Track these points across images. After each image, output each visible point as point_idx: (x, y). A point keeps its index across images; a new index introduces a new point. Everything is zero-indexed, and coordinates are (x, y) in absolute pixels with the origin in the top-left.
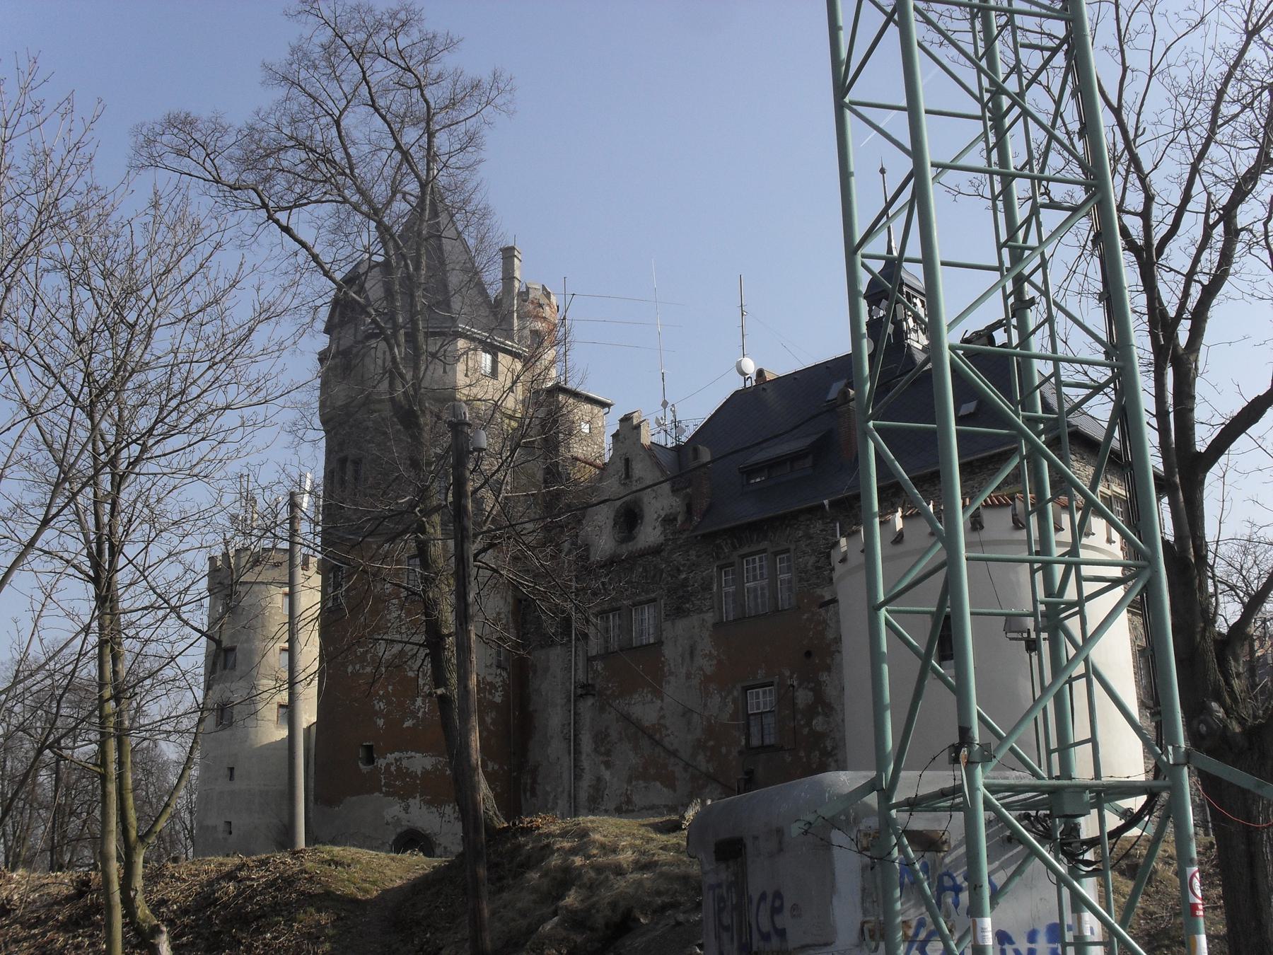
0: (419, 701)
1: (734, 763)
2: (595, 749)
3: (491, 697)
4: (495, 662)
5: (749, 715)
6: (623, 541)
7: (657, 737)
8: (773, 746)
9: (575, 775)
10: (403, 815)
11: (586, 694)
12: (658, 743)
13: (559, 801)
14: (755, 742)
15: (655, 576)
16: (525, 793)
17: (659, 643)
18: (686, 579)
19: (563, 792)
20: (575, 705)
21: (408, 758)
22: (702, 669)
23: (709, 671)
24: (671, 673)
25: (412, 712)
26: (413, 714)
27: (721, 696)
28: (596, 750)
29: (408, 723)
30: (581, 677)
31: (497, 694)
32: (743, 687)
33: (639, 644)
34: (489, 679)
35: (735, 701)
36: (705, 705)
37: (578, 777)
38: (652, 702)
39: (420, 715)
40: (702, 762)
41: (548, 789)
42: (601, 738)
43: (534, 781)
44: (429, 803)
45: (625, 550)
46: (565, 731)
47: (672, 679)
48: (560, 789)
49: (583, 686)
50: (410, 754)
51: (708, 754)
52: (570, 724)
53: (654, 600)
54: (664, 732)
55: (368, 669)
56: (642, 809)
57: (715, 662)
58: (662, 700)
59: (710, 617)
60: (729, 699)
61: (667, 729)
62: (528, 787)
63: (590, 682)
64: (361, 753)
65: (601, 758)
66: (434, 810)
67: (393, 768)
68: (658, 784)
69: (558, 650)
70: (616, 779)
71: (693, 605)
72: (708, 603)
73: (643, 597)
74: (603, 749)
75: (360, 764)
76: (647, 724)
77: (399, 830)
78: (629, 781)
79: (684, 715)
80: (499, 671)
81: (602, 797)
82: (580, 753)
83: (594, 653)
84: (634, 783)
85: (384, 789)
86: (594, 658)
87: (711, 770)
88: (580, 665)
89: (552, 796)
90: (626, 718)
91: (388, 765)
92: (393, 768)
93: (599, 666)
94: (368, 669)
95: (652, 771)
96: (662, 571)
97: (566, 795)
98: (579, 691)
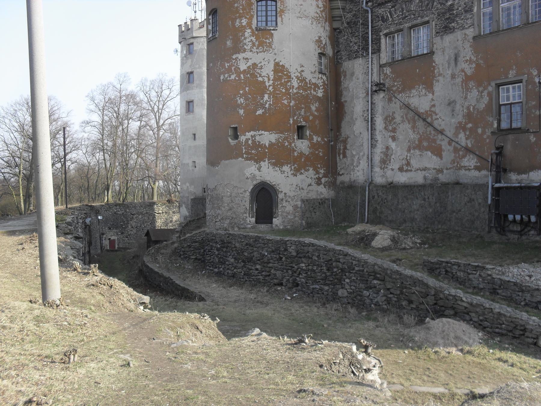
0: (266, 97)
1: (488, 141)
2: (385, 128)
3: (315, 93)
4: (317, 69)
5: (500, 106)
7: (429, 120)
8: (520, 129)
9: (372, 144)
10: (257, 172)
11: (380, 90)
12: (430, 125)
13: (360, 161)
14: (504, 125)
15: (428, 5)
16: (339, 156)
17: (432, 53)
18: (451, 5)
19: (364, 155)
20: (371, 97)
21: (260, 135)
22: (463, 71)
23: (469, 72)
24: (440, 75)
25: (262, 104)
26: (263, 106)
27: (478, 91)
28: (385, 128)
29: (260, 112)
30: (376, 79)
31: (319, 91)
32: (496, 84)
33: (416, 55)
34: (314, 81)
35: (490, 94)
36: (466, 98)
37: (373, 146)
38: (426, 95)
39: (267, 106)
40: (462, 138)
41: (354, 153)
42: (389, 120)
43: (345, 148)
44: (275, 165)
46: (365, 115)
47: (441, 78)
48: (361, 154)
49: (377, 85)
50: (261, 132)
51: (468, 133)
52: (368, 110)
53: (428, 22)
54: (434, 117)
55: (233, 77)
56: (418, 170)
57: (474, 65)
58: (433, 94)
59: (471, 32)
60: (485, 93)
61: (436, 115)
62: (341, 152)
63: (382, 82)
64: (230, 132)
65: (389, 134)
66: (277, 169)
67: (250, 142)
68: (429, 153)
69: (360, 61)
70: (399, 148)
71: (458, 23)
72: (469, 21)
73: (419, 20)
74: (390, 128)
75: (230, 140)
76: (422, 111)
77: (255, 183)
78: (409, 150)
79: (449, 104)
80: (320, 76)
81: (390, 160)
82: (375, 129)
84: (412, 151)
85: (245, 156)
86: (385, 65)
87: (470, 145)
88: (375, 70)
89: (357, 157)
90: (407, 106)
91: (247, 140)
92: (250, 142)
93: (388, 70)
94: (233, 77)
95: (425, 144)
97: (365, 157)
98: (374, 88)
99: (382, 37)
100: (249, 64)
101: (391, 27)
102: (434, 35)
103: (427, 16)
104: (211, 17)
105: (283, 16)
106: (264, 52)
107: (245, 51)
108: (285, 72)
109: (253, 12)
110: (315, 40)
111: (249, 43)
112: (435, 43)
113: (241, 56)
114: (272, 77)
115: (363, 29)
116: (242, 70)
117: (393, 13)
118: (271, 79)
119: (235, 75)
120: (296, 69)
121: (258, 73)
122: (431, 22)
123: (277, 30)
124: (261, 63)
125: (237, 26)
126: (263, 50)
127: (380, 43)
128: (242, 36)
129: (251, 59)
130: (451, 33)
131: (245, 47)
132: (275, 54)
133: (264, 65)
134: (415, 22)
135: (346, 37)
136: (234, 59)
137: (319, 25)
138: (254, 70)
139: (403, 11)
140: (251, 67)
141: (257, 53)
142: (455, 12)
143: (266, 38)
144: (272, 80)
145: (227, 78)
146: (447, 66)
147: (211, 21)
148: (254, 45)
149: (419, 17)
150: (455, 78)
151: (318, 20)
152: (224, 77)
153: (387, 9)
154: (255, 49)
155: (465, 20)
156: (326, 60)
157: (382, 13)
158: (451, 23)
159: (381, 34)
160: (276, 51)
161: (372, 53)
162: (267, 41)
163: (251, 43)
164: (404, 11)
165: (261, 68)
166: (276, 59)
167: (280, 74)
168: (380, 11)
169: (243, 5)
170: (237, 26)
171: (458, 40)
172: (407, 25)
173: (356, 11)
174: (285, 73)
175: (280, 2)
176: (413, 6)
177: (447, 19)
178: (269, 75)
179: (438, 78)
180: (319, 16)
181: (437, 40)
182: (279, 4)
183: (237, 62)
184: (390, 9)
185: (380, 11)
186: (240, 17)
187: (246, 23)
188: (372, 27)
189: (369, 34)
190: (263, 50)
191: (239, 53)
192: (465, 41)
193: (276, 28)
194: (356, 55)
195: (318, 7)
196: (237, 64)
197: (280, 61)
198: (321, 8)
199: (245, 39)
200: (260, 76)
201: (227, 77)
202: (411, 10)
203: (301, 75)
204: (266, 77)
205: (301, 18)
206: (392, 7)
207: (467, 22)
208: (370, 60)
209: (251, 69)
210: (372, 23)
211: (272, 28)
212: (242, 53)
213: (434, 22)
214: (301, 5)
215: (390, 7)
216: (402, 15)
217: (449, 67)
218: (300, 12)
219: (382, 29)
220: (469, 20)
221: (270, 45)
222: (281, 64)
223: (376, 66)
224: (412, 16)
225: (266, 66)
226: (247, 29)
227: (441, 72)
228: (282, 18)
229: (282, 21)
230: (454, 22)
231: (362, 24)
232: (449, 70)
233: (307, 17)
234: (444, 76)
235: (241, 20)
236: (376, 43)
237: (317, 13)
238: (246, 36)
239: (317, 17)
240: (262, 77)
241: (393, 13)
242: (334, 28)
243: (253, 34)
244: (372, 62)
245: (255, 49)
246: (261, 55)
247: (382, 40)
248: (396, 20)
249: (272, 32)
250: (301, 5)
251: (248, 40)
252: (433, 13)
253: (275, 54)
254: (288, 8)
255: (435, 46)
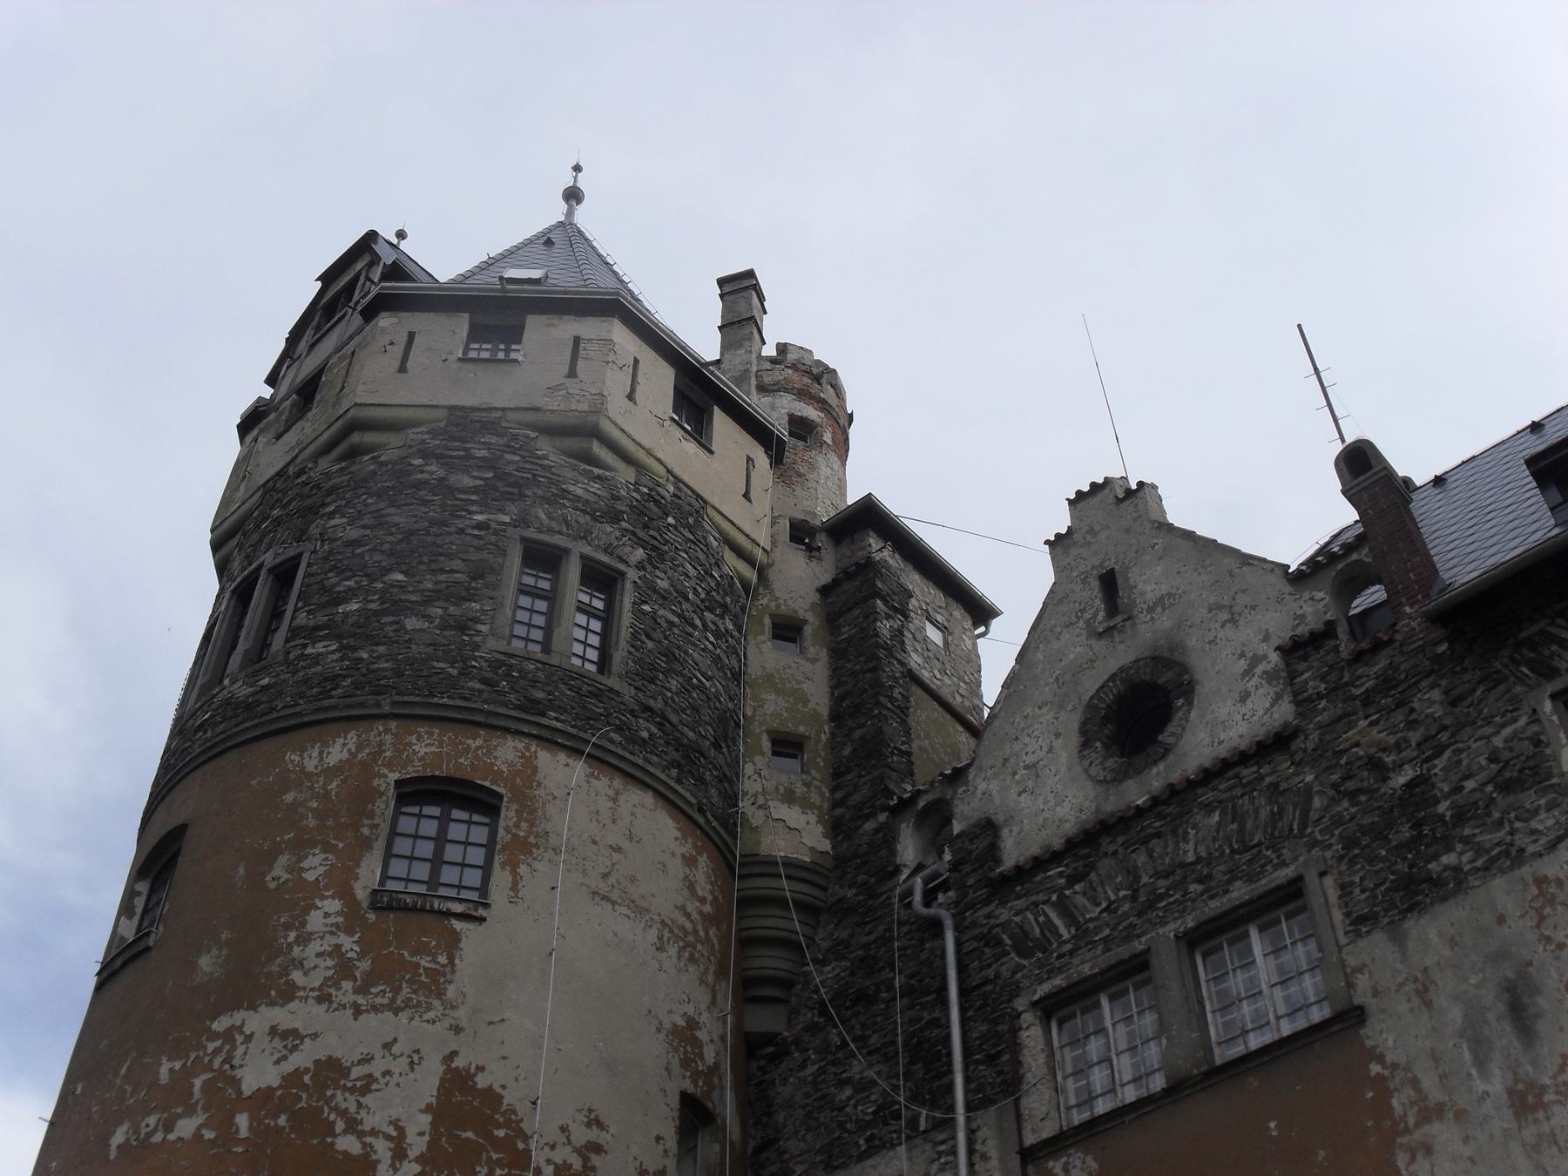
6: (1120, 776)
17: (1349, 1018)
18: (1410, 785)
24: (1430, 1113)
45: (1136, 793)
55: (186, 1127)
71: (1479, 851)
73: (1240, 892)
83: (1048, 1131)
94: (186, 1127)
96: (1308, 793)
99: (1027, 1018)
100: (302, 1059)
101: (1076, 961)
102: (1340, 933)
103: (1284, 864)
104: (143, 887)
105: (523, 869)
106: (397, 1011)
107: (289, 993)
108: (499, 1126)
109: (376, 826)
110: (667, 1025)
111: (320, 961)
112: (1360, 969)
113: (257, 1021)
114: (417, 1145)
115: (911, 1013)
116: (248, 1087)
117: (1081, 900)
118: (413, 1153)
119: (199, 1119)
120: (563, 1129)
121: (343, 1113)
122: (1312, 880)
123: (482, 920)
124: (367, 1060)
125: (273, 885)
126: (393, 1000)
127: (1015, 1047)
128: (288, 927)
129: (315, 1036)
130: (1445, 899)
131: (297, 976)
132: (457, 1029)
133: (387, 1073)
134: (1216, 905)
135: (811, 1070)
136: (215, 1036)
137: (692, 968)
138: (322, 1096)
139: (1137, 878)
140: (307, 1079)
141: (357, 1011)
142: (1442, 807)
143: (420, 950)
144: (420, 1159)
145: (150, 1135)
146: (1467, 1055)
147: (139, 903)
148: (344, 969)
149: (1230, 882)
150: (1540, 1105)
151: (688, 945)
152: (137, 1131)
153: (1041, 897)
154: (346, 992)
155: (1518, 825)
156: (717, 1147)
157: (1017, 919)
158: (1436, 857)
159: (1020, 1004)
160: (462, 1015)
161: (969, 1107)
162: (425, 962)
163: (330, 963)
164: (1145, 879)
165: (365, 1090)
166: (454, 1053)
167: (470, 1135)
168: (1004, 914)
169: (327, 793)
170: (273, 885)
171: (1501, 920)
172: (1170, 930)
173: (866, 946)
174: (501, 1133)
175: (514, 807)
176: (1190, 846)
177: (1405, 846)
178: (402, 1132)
179: (1418, 1135)
180: (696, 931)
181: (1376, 945)
182: (512, 814)
183: (234, 1048)
184: (1061, 889)
185: (1004, 914)
186: (301, 847)
187: (321, 870)
188: (962, 992)
189: (948, 1026)
190: (393, 1000)
191: (253, 1007)
192: (1547, 910)
193: (481, 912)
194: (869, 1140)
195: (691, 888)
196: (228, 1059)
197: (481, 1069)
198: (703, 900)
199: (305, 939)
200: (353, 1126)
201: (150, 1135)
202: (1183, 865)
203: (585, 1165)
204: (388, 1137)
205: (614, 903)
206: (1072, 880)
207: (1534, 824)
208: (961, 1136)
209: (305, 1087)
210: (962, 968)
211: (458, 908)
212: (272, 1004)
213: (1329, 881)
214: (618, 849)
215: (1062, 881)
216: (1134, 898)
217: (1481, 1063)
218: (606, 876)
219: (1025, 983)
220: (1543, 815)
221: (435, 985)
222: (482, 1081)
223: (994, 1163)
224: (1194, 888)
225: (396, 1078)
226: (323, 898)
227: (1436, 1094)
228: (514, 873)
229: (515, 887)
230: (1449, 849)
231: (907, 991)
232: (1484, 1073)
233: (638, 909)
234: (1460, 1115)
235: (301, 859)
236: (992, 1059)
237: (688, 915)
238: (309, 928)
239: (686, 933)
240: (360, 1135)
241: (1081, 900)
242: (747, 1035)
243: (352, 919)
244: (971, 1151)
245: (346, 992)
246: (379, 1026)
247: (1023, 1034)
248: (1098, 930)
249: (458, 925)
250: (618, 850)
251: (315, 946)
252: (1314, 844)
253: (457, 1029)
254: (553, 840)
255: (1362, 981)
